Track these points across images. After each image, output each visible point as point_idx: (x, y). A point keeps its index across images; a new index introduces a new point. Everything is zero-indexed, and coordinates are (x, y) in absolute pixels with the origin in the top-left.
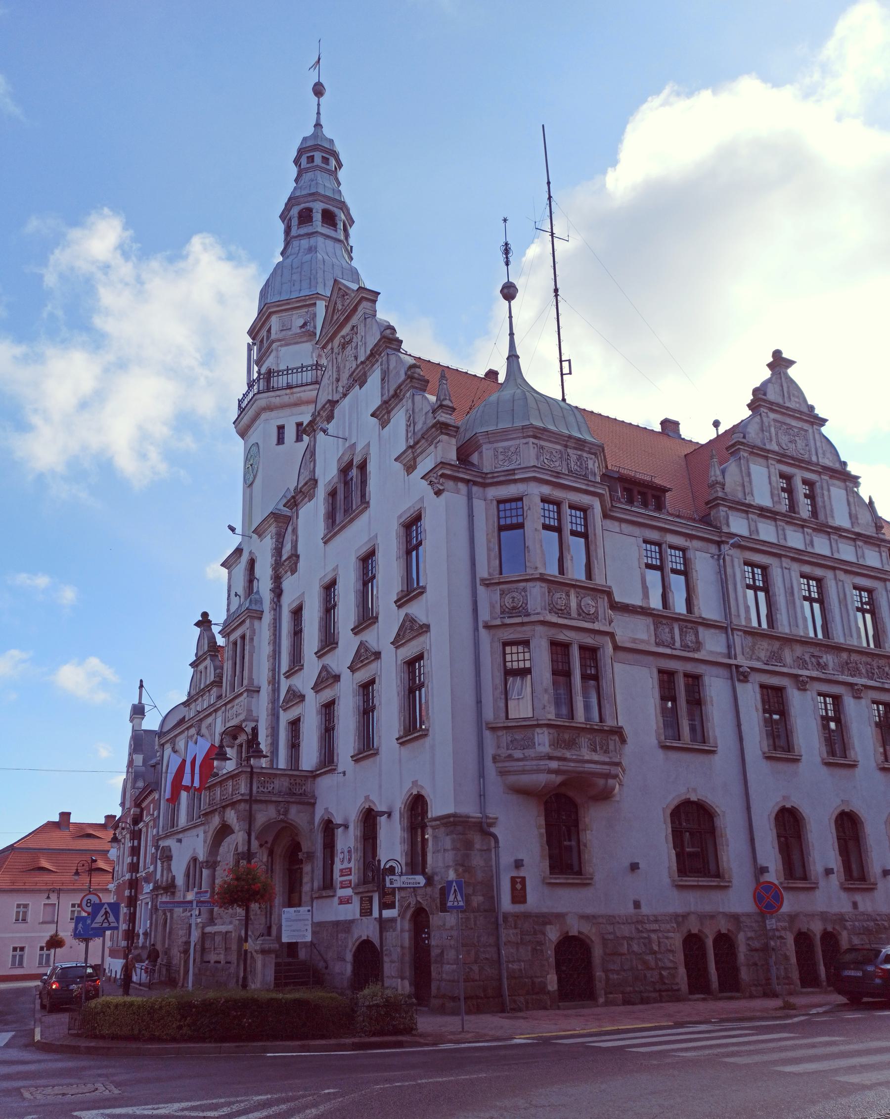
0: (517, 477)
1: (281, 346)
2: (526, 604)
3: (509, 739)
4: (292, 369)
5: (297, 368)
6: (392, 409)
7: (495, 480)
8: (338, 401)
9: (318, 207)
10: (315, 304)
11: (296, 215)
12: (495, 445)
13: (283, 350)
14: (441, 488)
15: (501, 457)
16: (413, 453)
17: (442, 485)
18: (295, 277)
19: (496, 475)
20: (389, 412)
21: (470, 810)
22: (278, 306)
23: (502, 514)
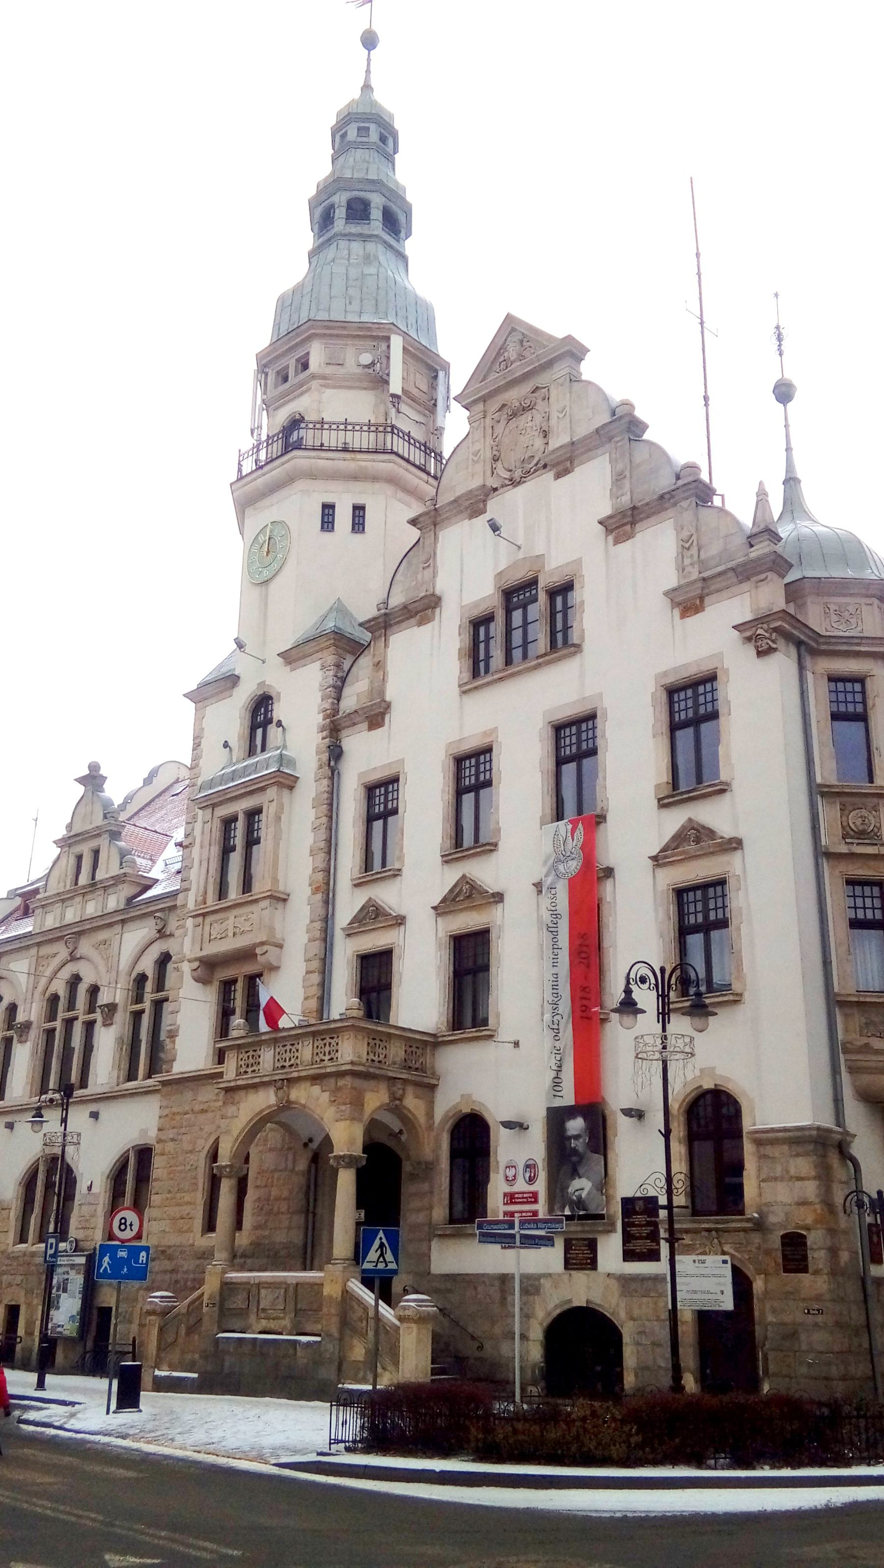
0: (863, 649)
1: (326, 386)
2: (879, 829)
3: (864, 1020)
4: (354, 425)
5: (362, 425)
6: (641, 520)
7: (831, 648)
8: (495, 490)
10: (388, 339)
12: (826, 599)
13: (329, 392)
14: (774, 646)
15: (834, 618)
16: (703, 588)
17: (774, 641)
19: (833, 640)
20: (633, 523)
21: (827, 1121)
22: (328, 328)
23: (858, 698)
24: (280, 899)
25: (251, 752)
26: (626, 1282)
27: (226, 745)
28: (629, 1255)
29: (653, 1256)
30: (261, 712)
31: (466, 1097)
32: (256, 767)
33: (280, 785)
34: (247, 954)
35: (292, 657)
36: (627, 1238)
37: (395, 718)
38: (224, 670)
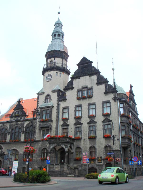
9: (61, 34)
11: (57, 34)
18: (59, 46)
24: (52, 121)
25: (45, 102)
26: (97, 165)
27: (43, 101)
28: (98, 162)
29: (101, 162)
30: (48, 98)
31: (78, 146)
32: (48, 105)
33: (52, 107)
34: (48, 127)
35: (53, 91)
36: (98, 161)
37: (68, 101)
38: (42, 91)
